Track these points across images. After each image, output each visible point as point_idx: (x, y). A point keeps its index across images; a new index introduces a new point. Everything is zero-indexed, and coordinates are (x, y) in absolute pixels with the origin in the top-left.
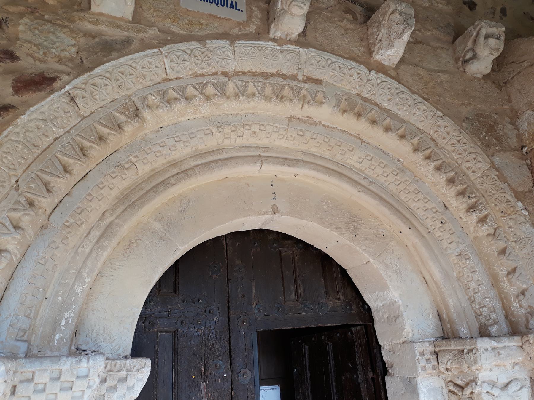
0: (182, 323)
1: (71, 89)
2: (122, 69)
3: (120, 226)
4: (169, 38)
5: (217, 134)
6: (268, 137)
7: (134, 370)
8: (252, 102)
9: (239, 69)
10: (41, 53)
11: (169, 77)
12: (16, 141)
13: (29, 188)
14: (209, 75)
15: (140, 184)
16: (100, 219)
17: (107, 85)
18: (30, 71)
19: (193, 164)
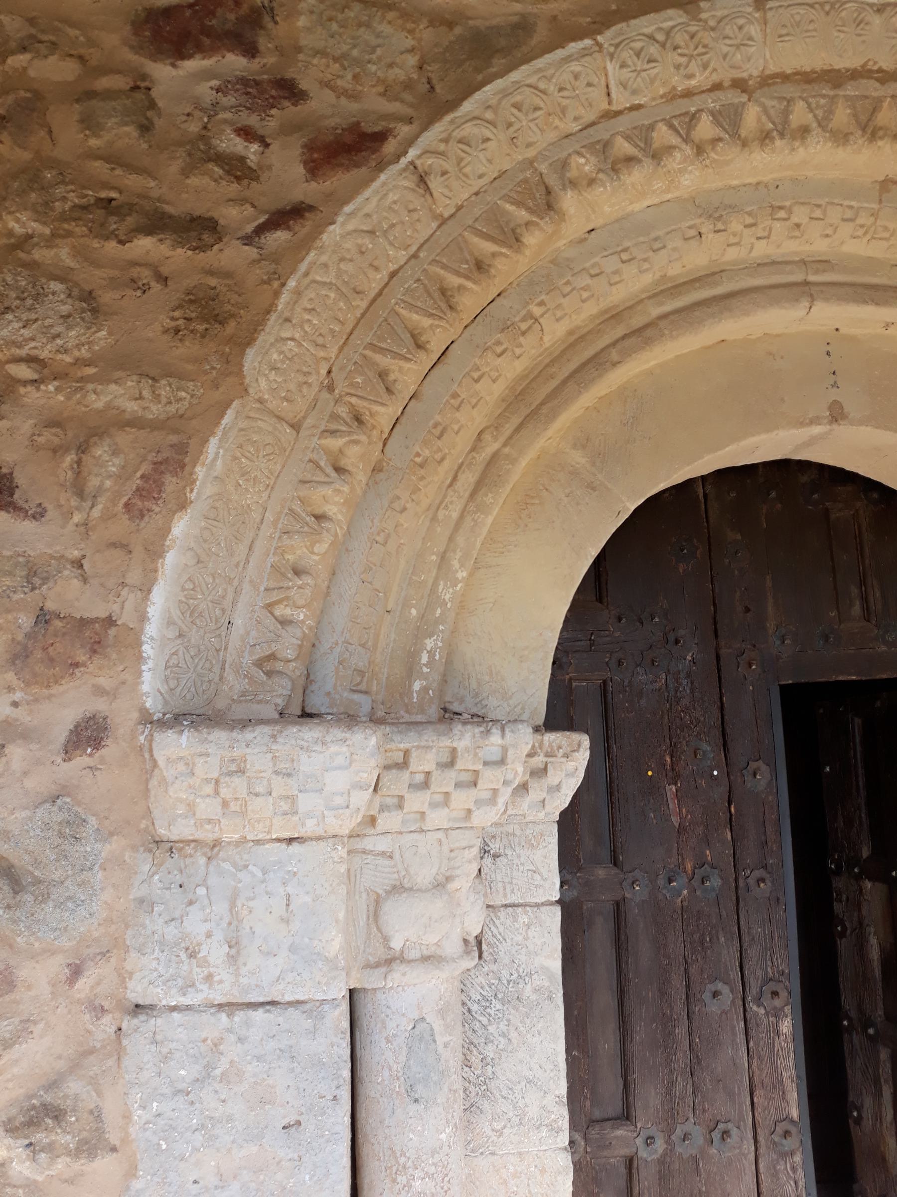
0: (620, 663)
1: (419, 157)
2: (518, 98)
3: (514, 461)
4: (614, 7)
5: (711, 236)
6: (827, 236)
8: (801, 149)
9: (772, 69)
10: (349, 77)
11: (614, 108)
12: (325, 284)
13: (352, 385)
14: (703, 92)
15: (547, 366)
16: (473, 449)
17: (488, 139)
18: (331, 122)
19: (656, 311)
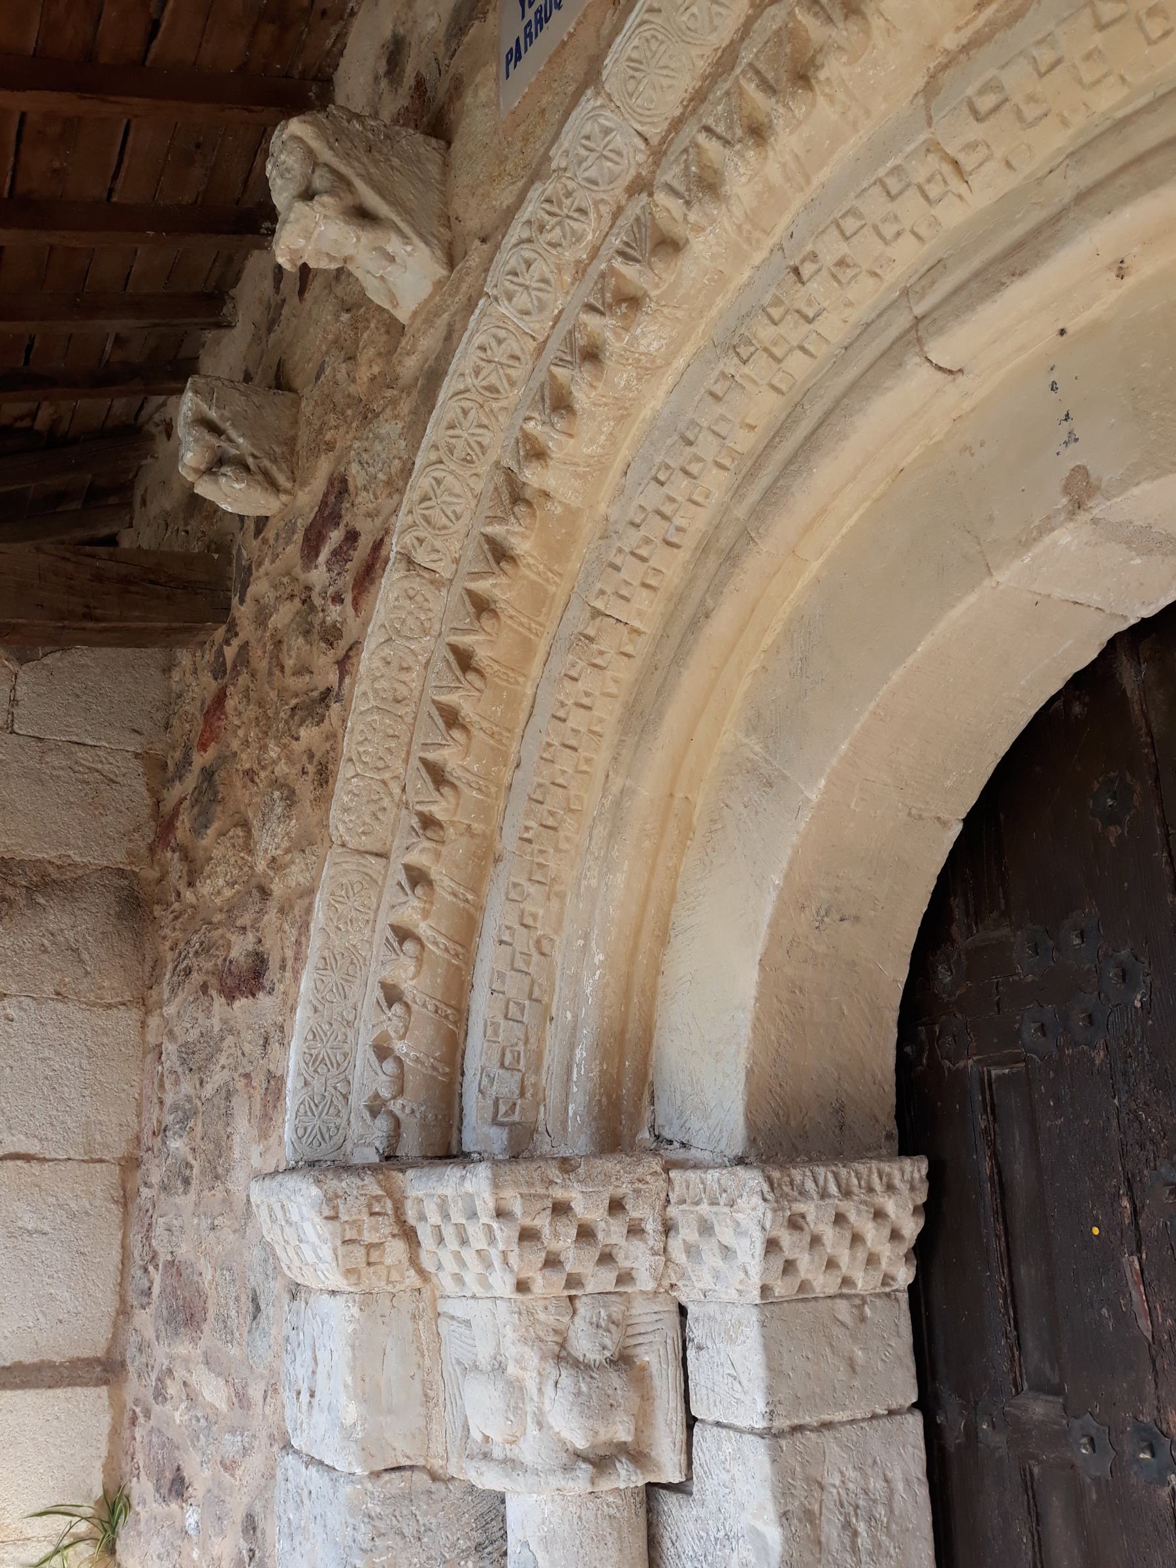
5: (746, 370)
7: (722, 1201)
9: (655, 132)
11: (541, 339)
